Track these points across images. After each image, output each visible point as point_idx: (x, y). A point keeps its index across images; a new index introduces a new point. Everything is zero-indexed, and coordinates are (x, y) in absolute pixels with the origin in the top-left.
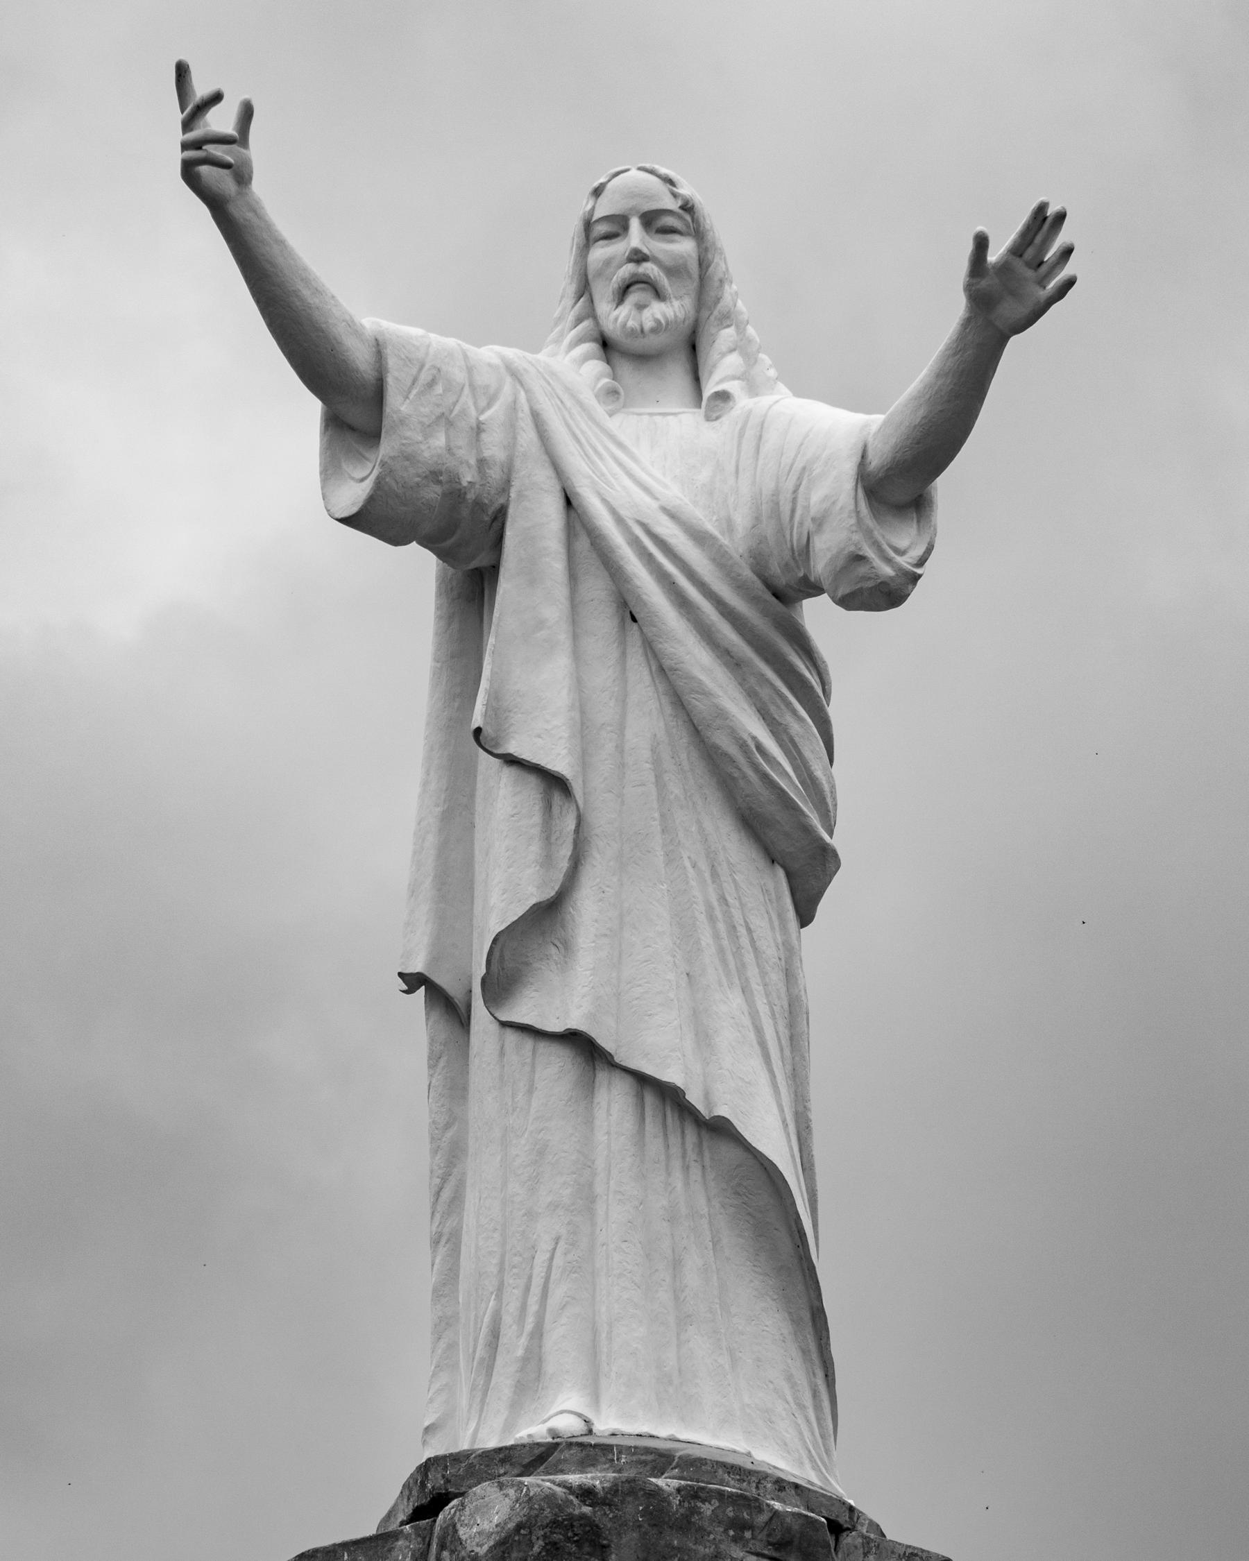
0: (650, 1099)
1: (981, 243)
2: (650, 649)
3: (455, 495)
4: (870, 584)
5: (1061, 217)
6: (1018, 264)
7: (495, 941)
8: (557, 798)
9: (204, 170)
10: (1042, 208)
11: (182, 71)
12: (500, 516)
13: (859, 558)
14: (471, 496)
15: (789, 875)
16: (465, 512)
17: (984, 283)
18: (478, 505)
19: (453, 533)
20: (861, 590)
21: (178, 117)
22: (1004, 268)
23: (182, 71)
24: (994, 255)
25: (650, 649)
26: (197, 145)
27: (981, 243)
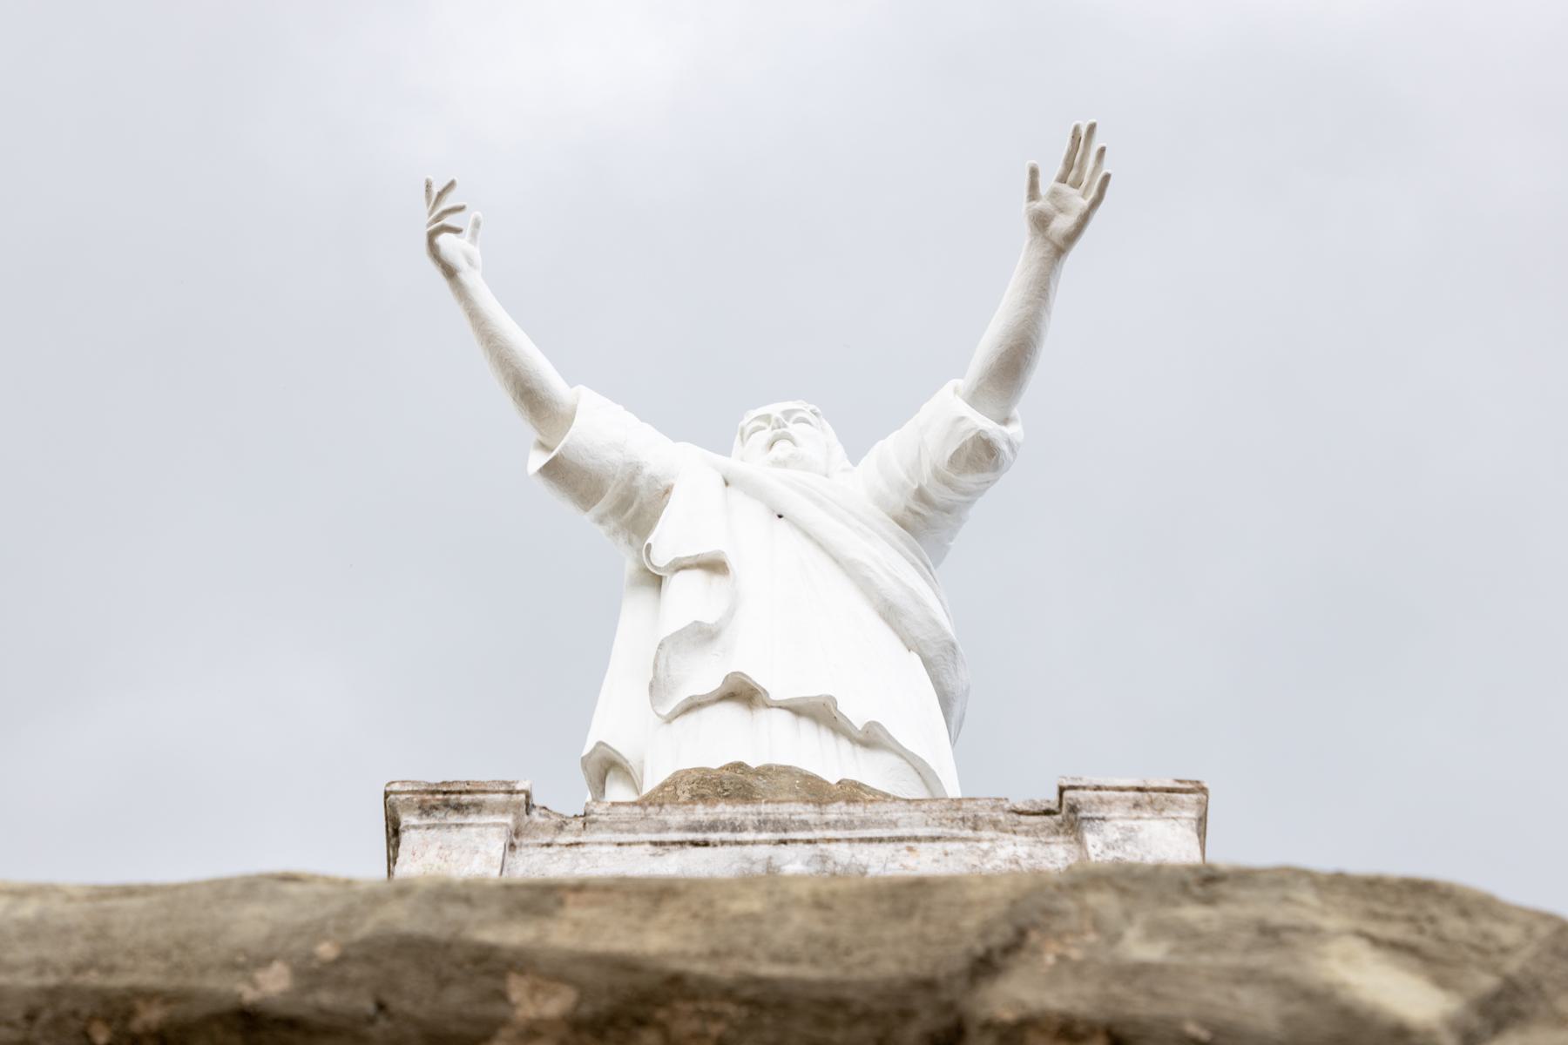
0: (806, 725)
1: (1034, 173)
2: (797, 525)
3: (635, 470)
4: (973, 433)
5: (1092, 128)
6: (1065, 188)
7: (661, 646)
8: (717, 580)
9: (444, 240)
10: (1076, 129)
11: (428, 186)
12: (667, 491)
13: (962, 419)
14: (646, 471)
15: (927, 663)
16: (641, 481)
17: (1038, 205)
18: (654, 479)
19: (631, 504)
20: (964, 444)
21: (426, 210)
22: (1054, 194)
23: (428, 186)
24: (1047, 183)
25: (797, 525)
26: (438, 219)
27: (1034, 173)
